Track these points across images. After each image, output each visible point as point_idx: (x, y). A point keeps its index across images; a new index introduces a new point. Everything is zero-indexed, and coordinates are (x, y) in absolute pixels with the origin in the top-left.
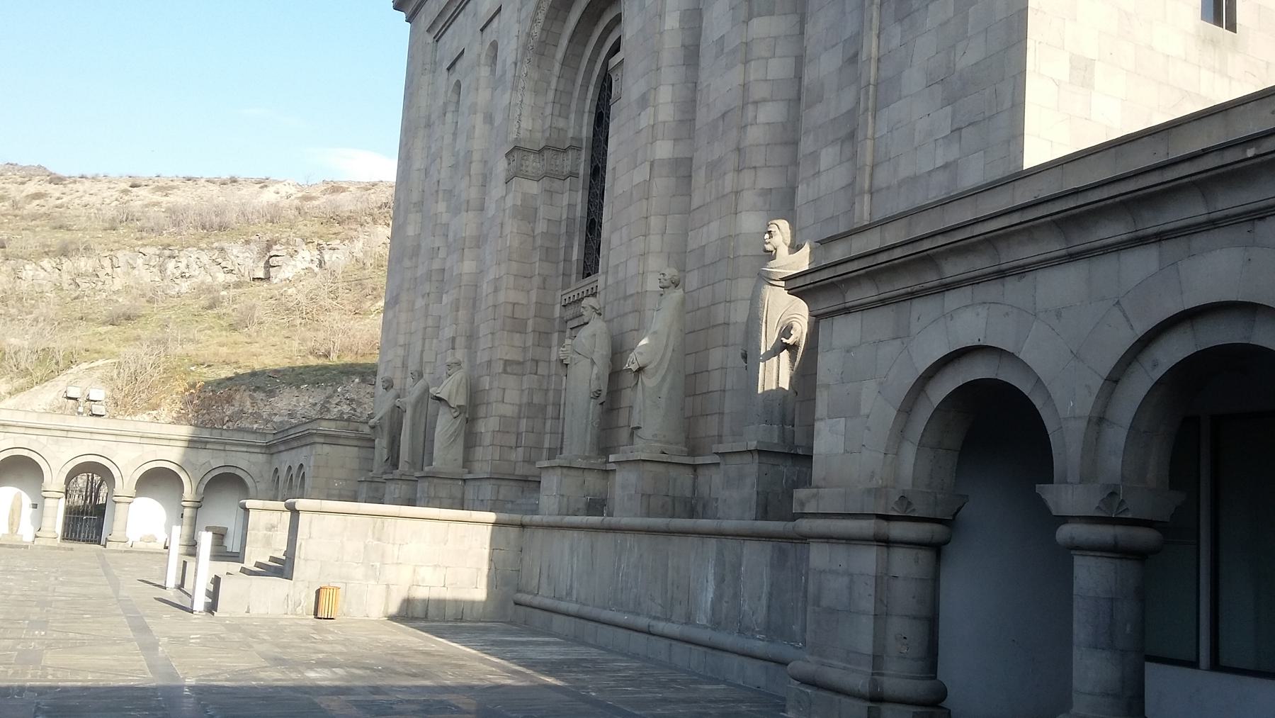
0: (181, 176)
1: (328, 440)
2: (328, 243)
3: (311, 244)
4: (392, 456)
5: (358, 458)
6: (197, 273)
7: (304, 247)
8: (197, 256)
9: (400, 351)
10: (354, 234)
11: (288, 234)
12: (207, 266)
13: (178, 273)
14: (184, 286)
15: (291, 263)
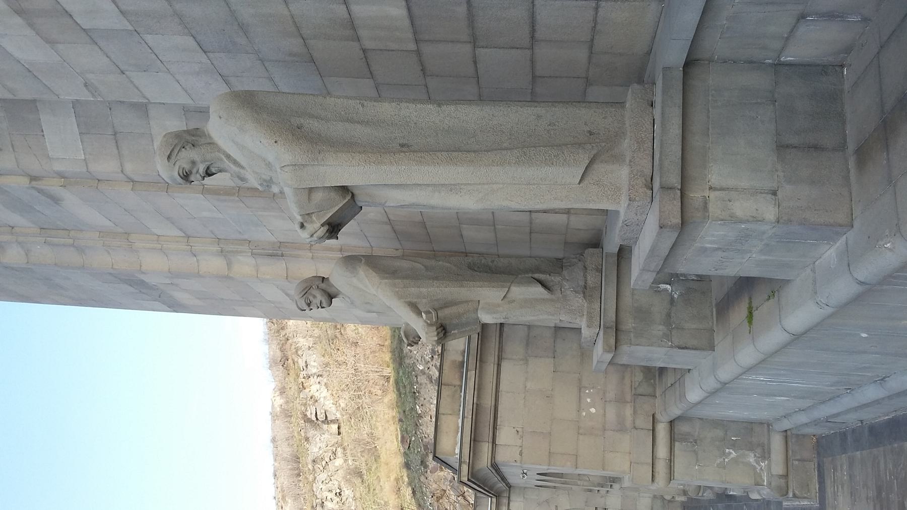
0: (273, 481)
1: (486, 433)
2: (302, 370)
3: (305, 385)
4: (526, 271)
5: (526, 360)
6: (336, 483)
7: (307, 390)
8: (320, 483)
9: (245, 265)
10: (293, 347)
11: (298, 405)
12: (329, 474)
13: (337, 499)
14: (347, 492)
15: (322, 402)
